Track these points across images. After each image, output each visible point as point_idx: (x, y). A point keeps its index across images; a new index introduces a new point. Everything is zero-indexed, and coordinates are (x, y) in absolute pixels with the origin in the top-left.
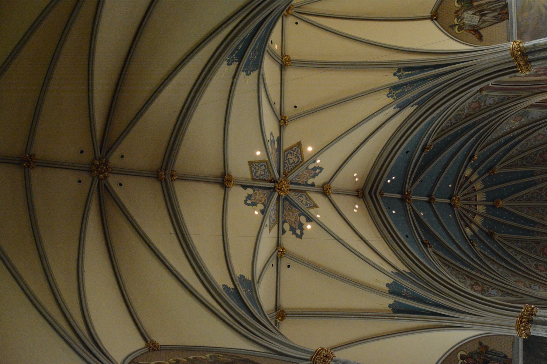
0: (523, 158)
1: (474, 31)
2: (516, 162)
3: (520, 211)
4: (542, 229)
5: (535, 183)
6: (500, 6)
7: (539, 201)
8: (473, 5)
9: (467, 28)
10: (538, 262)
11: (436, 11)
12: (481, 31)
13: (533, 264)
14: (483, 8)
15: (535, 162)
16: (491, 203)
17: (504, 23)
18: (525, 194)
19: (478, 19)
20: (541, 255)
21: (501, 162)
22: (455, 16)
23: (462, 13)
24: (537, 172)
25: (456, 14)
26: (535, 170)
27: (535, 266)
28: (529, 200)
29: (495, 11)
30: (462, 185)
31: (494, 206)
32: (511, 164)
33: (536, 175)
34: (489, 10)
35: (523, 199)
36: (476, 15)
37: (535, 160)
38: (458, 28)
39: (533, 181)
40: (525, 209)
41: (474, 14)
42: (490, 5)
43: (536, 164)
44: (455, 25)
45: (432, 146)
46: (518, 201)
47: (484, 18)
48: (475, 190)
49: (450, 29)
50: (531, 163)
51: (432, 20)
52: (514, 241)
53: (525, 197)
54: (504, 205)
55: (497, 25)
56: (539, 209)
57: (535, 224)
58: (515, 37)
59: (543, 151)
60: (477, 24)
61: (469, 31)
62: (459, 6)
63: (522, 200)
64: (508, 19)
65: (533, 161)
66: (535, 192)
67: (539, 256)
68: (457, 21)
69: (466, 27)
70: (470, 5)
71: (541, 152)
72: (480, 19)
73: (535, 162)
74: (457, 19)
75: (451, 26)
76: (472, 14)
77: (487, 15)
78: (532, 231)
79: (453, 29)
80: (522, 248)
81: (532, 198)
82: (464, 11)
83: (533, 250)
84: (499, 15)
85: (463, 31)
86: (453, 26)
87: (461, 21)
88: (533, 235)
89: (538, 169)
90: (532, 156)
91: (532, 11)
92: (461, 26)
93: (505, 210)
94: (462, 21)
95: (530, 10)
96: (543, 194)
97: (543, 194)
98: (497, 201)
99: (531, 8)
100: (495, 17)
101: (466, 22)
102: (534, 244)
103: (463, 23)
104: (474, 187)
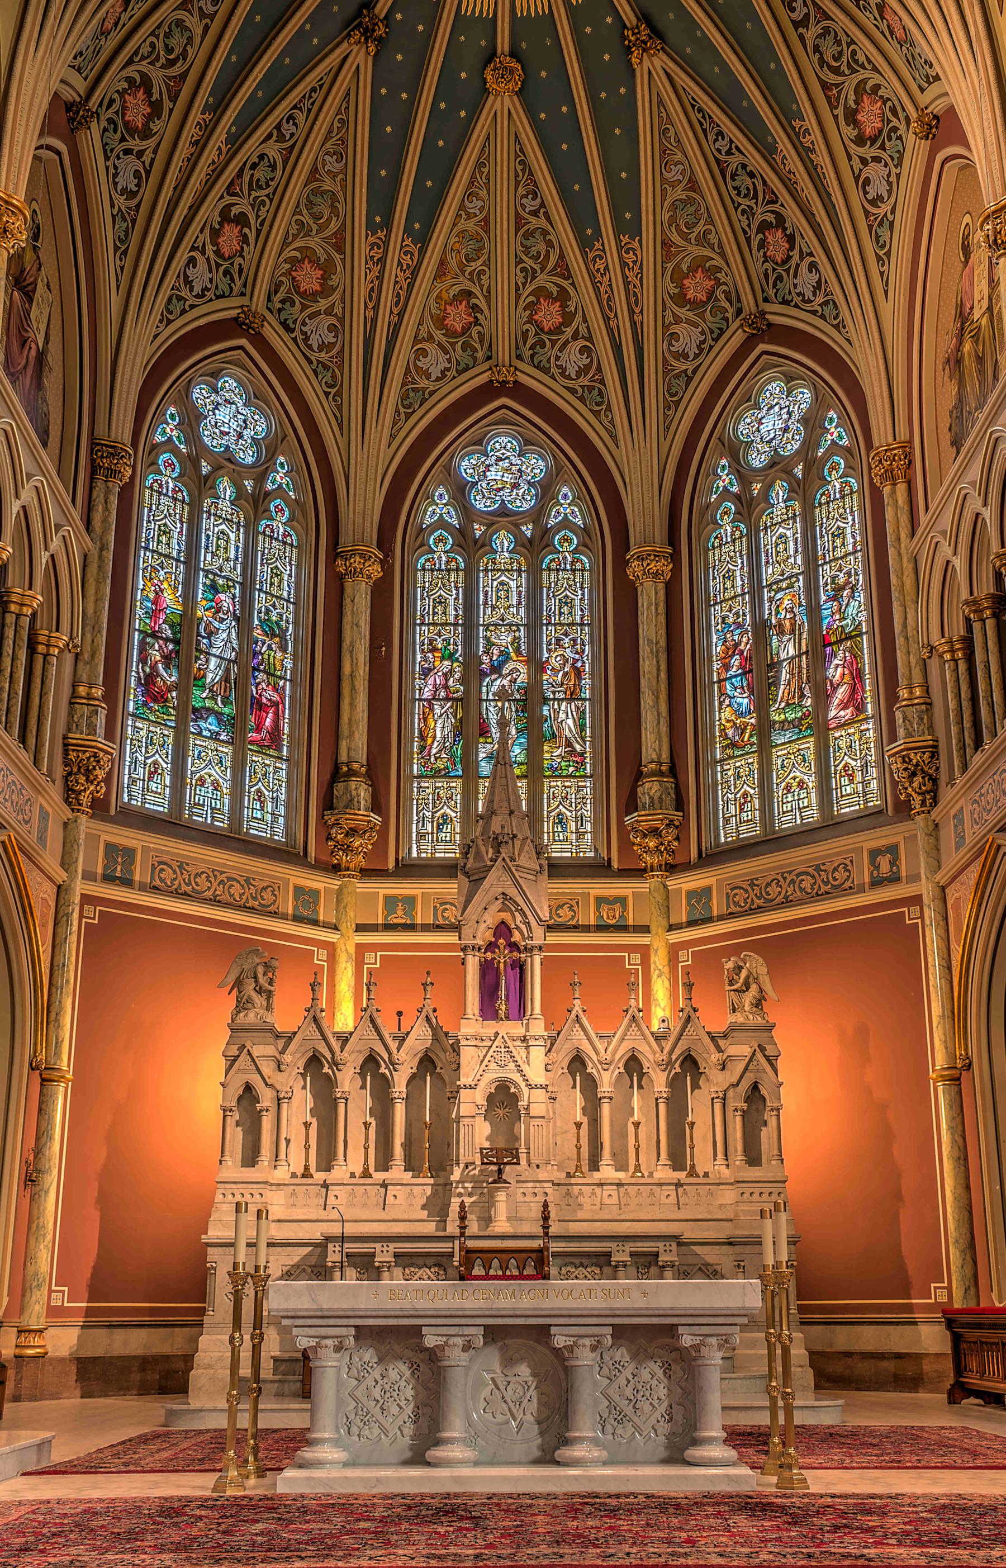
0: (693, 185)
2: (679, 156)
3: (472, 183)
4: (400, 263)
5: (585, 244)
7: (517, 264)
10: (259, 232)
13: (242, 206)
15: (676, 238)
16: (503, 43)
18: (543, 205)
20: (287, 254)
21: (682, 79)
24: (633, 250)
26: (640, 242)
27: (234, 211)
28: (519, 222)
31: (491, 56)
32: (672, 133)
33: (619, 248)
35: (523, 197)
37: (685, 237)
39: (598, 234)
40: (480, 203)
43: (666, 244)
46: (517, 176)
50: (670, 225)
52: (343, 141)
53: (531, 204)
54: (498, 105)
56: (480, 261)
57: (423, 239)
59: (719, 269)
63: (521, 191)
65: (679, 231)
66: (550, 244)
67: (285, 244)
71: (718, 261)
73: (676, 238)
78: (387, 224)
80: (314, 170)
81: (528, 235)
83: (311, 222)
88: (371, 227)
89: (648, 250)
90: (700, 228)
93: (474, 114)
96: (542, 279)
97: (542, 279)
98: (512, 72)
102: (334, 226)
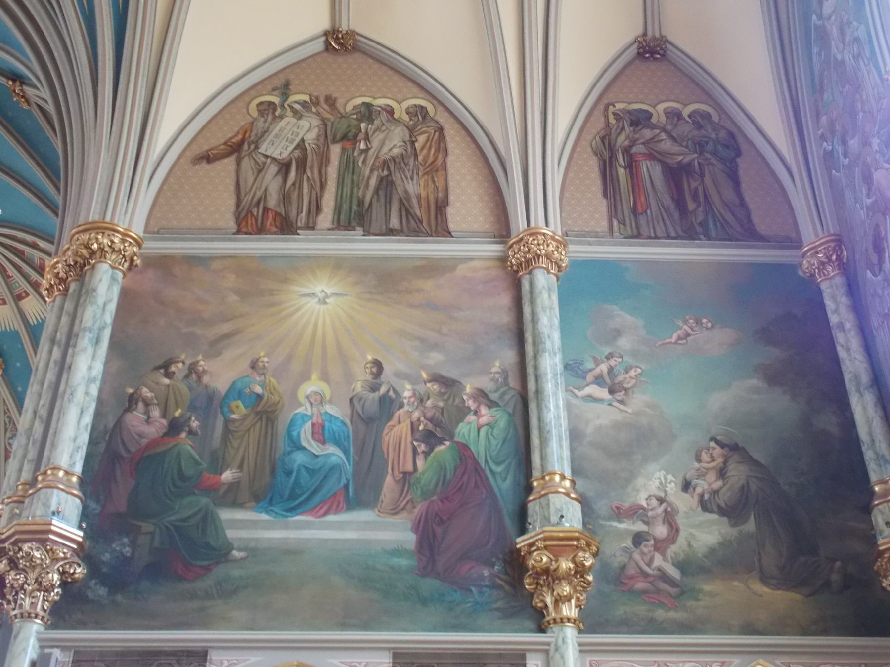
1: (240, 144)
6: (293, 213)
8: (335, 141)
9: (260, 124)
11: (356, 49)
12: (229, 163)
14: (312, 168)
17: (232, 225)
19: (276, 155)
22: (317, 98)
23: (318, 114)
25: (322, 100)
29: (285, 198)
30: (20, 254)
34: (294, 184)
36: (297, 147)
38: (271, 103)
41: (301, 146)
42: (311, 188)
44: (285, 95)
45: (25, 106)
47: (274, 169)
48: (18, 298)
49: (278, 82)
51: (326, 34)
55: (232, 201)
58: (156, 247)
60: (262, 150)
61: (246, 131)
62: (349, 108)
64: (239, 232)
68: (296, 102)
69: (265, 121)
70: (338, 137)
72: (274, 159)
74: (305, 102)
75: (287, 85)
76: (303, 140)
77: (280, 179)
79: (274, 90)
82: (324, 121)
84: (266, 210)
85: (254, 113)
86: (285, 90)
87: (295, 112)
91: (233, 298)
92: (275, 110)
94: (289, 113)
95: (238, 292)
99: (243, 295)
100: (265, 197)
101: (282, 123)
103: (281, 117)
104: (27, 295)
